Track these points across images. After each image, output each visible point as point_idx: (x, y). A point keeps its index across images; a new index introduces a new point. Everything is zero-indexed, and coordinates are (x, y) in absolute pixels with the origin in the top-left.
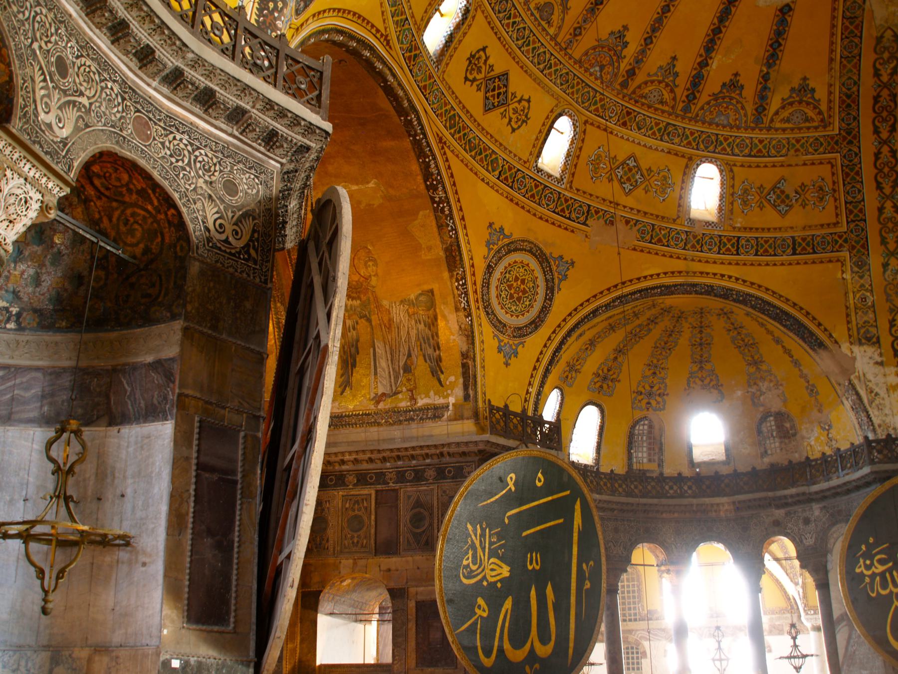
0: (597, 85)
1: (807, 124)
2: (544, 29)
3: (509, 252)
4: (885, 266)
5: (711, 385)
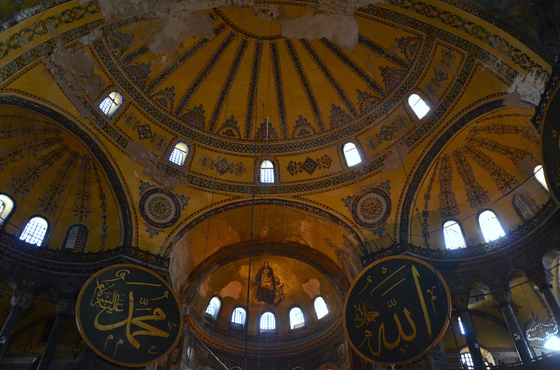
1: (418, 46)
2: (308, 136)
3: (358, 200)
4: (491, 44)
5: (522, 155)
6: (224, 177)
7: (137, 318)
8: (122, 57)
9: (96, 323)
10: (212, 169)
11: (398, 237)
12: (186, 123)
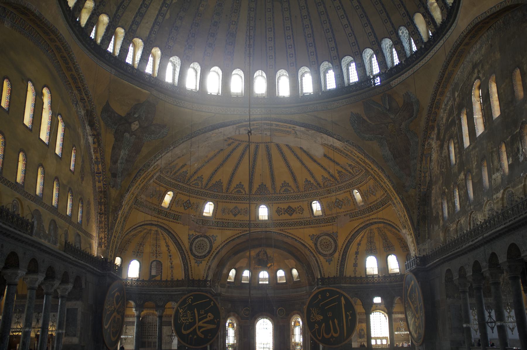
2: (290, 193)
3: (319, 238)
6: (236, 218)
7: (201, 322)
8: (172, 174)
9: (183, 331)
11: (338, 268)
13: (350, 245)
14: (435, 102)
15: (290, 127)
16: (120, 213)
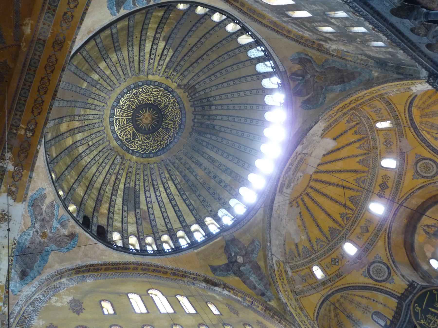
0: (371, 160)
3: (418, 172)
4: (383, 90)
8: (298, 258)
10: (364, 235)
12: (335, 238)
13: (432, 146)
14: (296, 39)
15: (297, 156)
16: (289, 308)
